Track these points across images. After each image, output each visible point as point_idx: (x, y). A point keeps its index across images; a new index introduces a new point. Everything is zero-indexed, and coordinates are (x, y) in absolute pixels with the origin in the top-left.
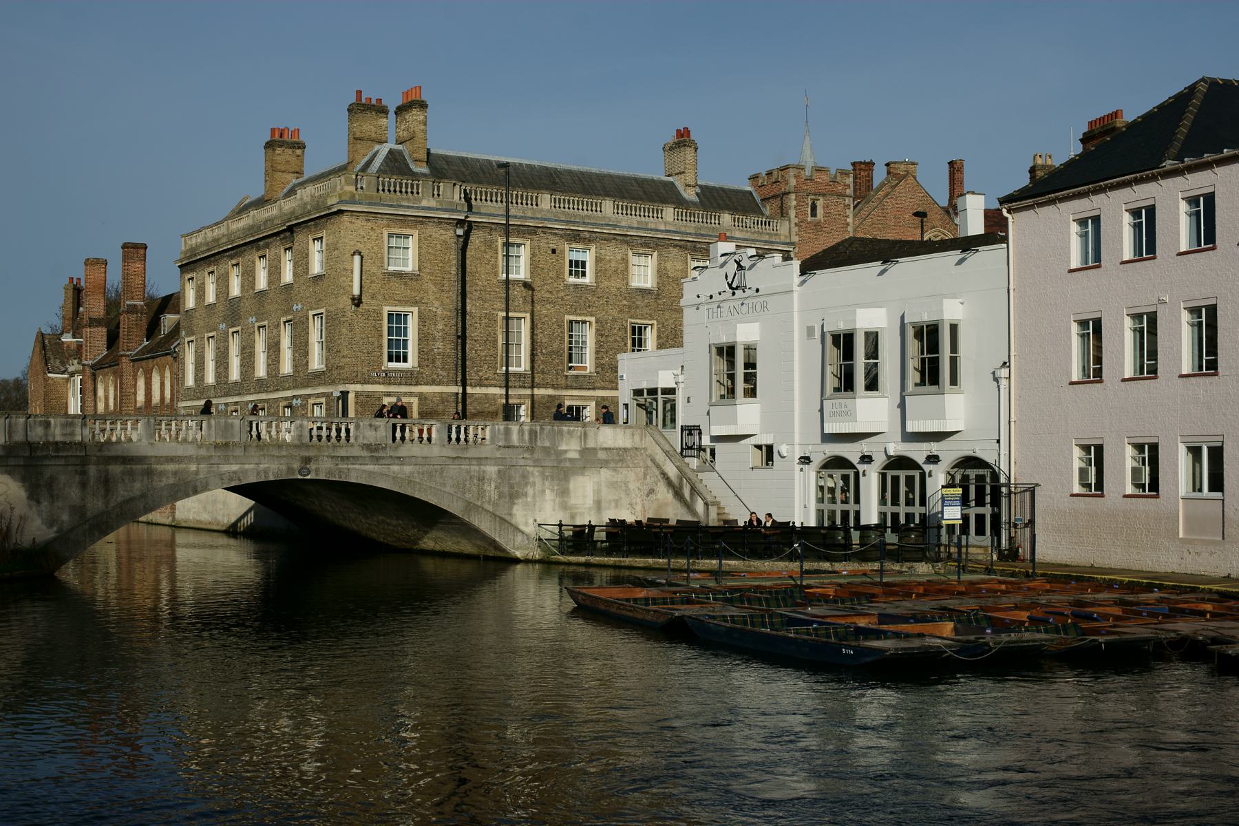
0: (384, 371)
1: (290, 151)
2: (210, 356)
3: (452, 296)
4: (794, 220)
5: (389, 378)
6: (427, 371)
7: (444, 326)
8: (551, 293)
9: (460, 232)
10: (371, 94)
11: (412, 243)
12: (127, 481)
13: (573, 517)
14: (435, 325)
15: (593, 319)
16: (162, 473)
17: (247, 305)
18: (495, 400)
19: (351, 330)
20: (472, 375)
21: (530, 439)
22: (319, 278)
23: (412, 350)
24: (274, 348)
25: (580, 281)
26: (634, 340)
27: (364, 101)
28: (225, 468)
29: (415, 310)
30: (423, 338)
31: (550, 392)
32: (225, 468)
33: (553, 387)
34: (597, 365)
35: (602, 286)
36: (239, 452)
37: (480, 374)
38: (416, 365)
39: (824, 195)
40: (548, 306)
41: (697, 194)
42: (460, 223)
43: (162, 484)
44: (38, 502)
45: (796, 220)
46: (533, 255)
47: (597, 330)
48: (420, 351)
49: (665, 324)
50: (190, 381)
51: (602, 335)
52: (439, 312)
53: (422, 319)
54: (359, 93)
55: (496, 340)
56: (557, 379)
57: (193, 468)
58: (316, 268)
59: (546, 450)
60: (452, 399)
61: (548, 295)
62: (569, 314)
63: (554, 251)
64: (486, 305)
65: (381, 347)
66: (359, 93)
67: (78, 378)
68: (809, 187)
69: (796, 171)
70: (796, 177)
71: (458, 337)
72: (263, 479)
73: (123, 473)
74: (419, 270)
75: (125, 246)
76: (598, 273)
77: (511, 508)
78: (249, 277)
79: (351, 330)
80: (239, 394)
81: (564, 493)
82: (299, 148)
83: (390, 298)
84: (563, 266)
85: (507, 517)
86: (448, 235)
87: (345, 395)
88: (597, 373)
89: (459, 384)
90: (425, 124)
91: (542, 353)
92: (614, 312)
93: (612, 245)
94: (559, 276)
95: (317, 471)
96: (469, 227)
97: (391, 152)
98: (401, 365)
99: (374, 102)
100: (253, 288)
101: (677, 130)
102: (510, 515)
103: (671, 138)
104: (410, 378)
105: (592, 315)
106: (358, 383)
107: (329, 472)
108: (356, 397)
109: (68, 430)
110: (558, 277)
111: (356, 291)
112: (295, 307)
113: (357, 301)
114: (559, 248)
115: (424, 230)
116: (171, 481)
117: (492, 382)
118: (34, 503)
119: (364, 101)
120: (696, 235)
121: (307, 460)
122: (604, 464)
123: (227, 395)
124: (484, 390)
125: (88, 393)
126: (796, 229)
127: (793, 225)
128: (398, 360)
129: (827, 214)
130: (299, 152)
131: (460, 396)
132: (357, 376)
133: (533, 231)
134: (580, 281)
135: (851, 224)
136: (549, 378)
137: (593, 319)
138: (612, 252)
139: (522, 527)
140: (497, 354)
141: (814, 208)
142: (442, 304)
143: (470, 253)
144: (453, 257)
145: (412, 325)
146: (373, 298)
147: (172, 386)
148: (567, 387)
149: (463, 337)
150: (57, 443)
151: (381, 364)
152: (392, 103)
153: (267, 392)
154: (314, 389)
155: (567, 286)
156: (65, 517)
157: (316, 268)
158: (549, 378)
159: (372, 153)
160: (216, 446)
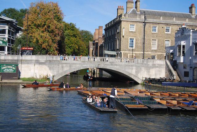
2: (110, 45)
5: (129, 50)
6: (137, 49)
9: (144, 24)
13: (150, 76)
15: (170, 40)
16: (73, 66)
22: (119, 32)
25: (168, 33)
28: (84, 65)
30: (136, 43)
31: (161, 53)
32: (84, 65)
36: (86, 63)
42: (144, 22)
44: (51, 70)
57: (78, 65)
59: (145, 64)
63: (163, 27)
65: (128, 45)
73: (66, 66)
75: (99, 27)
81: (149, 72)
86: (142, 24)
94: (163, 32)
96: (145, 23)
97: (133, 10)
107: (103, 67)
109: (56, 58)
118: (50, 70)
120: (192, 24)
121: (99, 65)
122: (157, 67)
124: (148, 53)
130: (123, 10)
134: (168, 33)
137: (170, 40)
139: (140, 78)
142: (140, 37)
143: (145, 28)
145: (134, 41)
149: (144, 43)
156: (55, 73)
160: (82, 62)
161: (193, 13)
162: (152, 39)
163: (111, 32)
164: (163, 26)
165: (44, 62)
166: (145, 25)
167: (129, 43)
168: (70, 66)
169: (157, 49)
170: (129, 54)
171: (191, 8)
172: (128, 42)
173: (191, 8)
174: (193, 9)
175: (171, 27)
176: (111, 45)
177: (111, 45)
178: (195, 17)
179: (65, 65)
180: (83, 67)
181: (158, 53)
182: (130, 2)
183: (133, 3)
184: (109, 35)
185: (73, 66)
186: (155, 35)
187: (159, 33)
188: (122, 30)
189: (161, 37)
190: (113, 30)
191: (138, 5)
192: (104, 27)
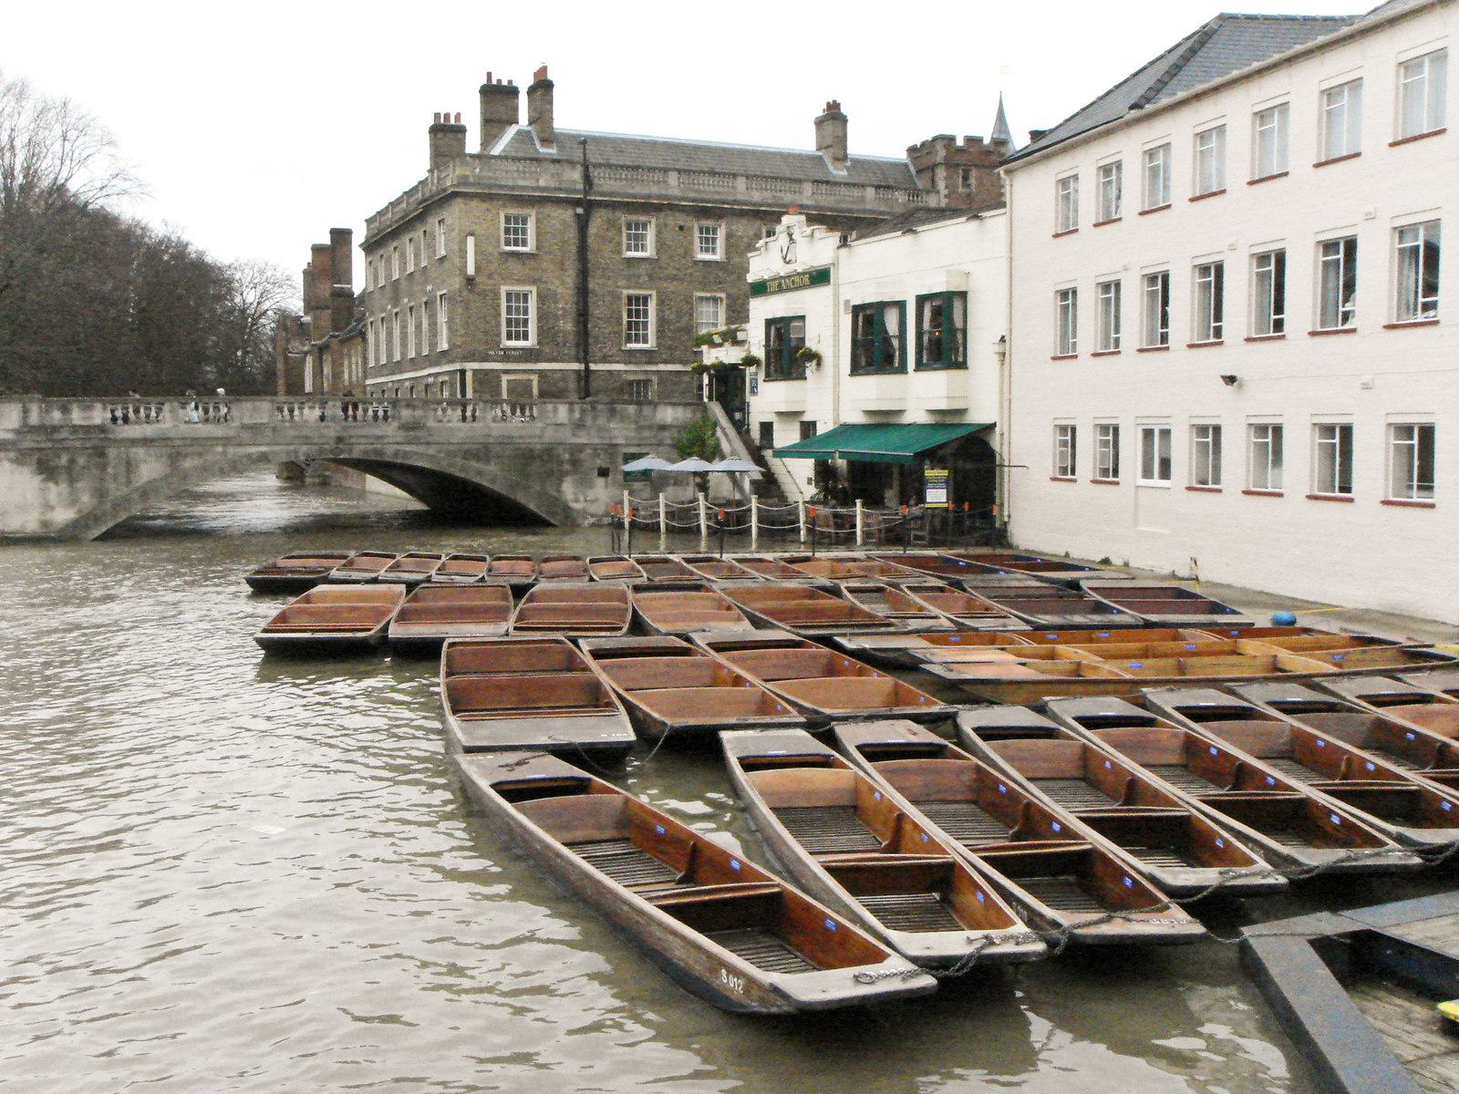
0: (502, 349)
2: (397, 333)
3: (571, 277)
4: (944, 191)
5: (507, 356)
10: (502, 76)
11: (531, 226)
15: (723, 295)
17: (404, 285)
18: (619, 376)
20: (593, 349)
24: (419, 326)
27: (494, 82)
29: (534, 289)
37: (604, 350)
39: (976, 166)
41: (848, 169)
42: (577, 203)
45: (946, 192)
50: (371, 363)
51: (734, 311)
53: (542, 298)
54: (489, 75)
55: (620, 318)
57: (220, 449)
60: (573, 376)
63: (681, 228)
64: (610, 283)
65: (498, 325)
66: (489, 75)
67: (309, 359)
69: (946, 142)
74: (538, 248)
83: (508, 278)
86: (567, 215)
87: (463, 372)
93: (744, 221)
94: (688, 252)
95: (351, 451)
96: (590, 206)
97: (519, 133)
98: (521, 344)
99: (505, 83)
102: (558, 491)
103: (819, 111)
104: (529, 355)
105: (722, 290)
106: (475, 361)
108: (474, 375)
111: (471, 270)
113: (470, 281)
114: (689, 224)
119: (494, 82)
123: (393, 373)
125: (318, 372)
128: (517, 338)
129: (980, 185)
130: (460, 136)
133: (658, 208)
137: (723, 295)
138: (743, 228)
140: (621, 331)
141: (966, 178)
142: (563, 283)
144: (572, 234)
150: (74, 426)
152: (524, 82)
155: (696, 263)
156: (86, 499)
162: (626, 292)
163: (403, 256)
164: (681, 219)
165: (10, 436)
167: (504, 316)
168: (175, 458)
170: (505, 378)
172: (497, 307)
175: (723, 226)
176: (404, 328)
177: (404, 328)
179: (139, 452)
181: (662, 367)
184: (388, 276)
186: (643, 270)
187: (664, 257)
189: (675, 278)
190: (410, 250)
192: (359, 237)
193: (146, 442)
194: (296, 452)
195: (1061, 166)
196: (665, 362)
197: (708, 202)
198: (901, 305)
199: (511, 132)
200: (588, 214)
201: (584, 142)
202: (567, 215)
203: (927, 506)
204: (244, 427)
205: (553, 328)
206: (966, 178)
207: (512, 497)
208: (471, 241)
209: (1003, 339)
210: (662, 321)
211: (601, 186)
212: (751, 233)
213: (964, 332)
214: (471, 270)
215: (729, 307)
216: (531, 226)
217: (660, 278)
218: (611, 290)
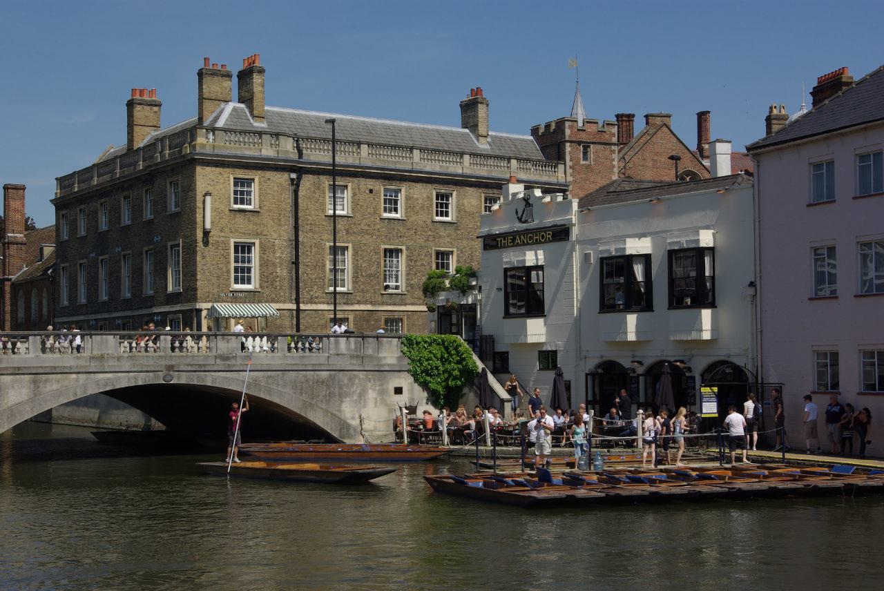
1: (148, 108)
2: (81, 280)
3: (287, 231)
5: (236, 297)
6: (267, 291)
7: (283, 253)
8: (369, 226)
10: (217, 61)
12: (16, 387)
14: (274, 252)
19: (204, 258)
20: (304, 294)
21: (356, 348)
22: (175, 216)
23: (255, 274)
24: (137, 274)
25: (393, 215)
26: (437, 264)
27: (211, 67)
29: (257, 242)
30: (264, 264)
31: (369, 307)
33: (371, 303)
34: (408, 285)
35: (411, 220)
37: (311, 293)
38: (258, 286)
39: (593, 143)
40: (367, 237)
41: (489, 143)
43: (47, 390)
45: (571, 164)
46: (354, 195)
47: (407, 256)
48: (262, 275)
49: (464, 250)
51: (411, 260)
52: (277, 242)
53: (263, 249)
55: (324, 266)
56: (375, 297)
57: (74, 376)
58: (173, 208)
61: (367, 228)
62: (384, 243)
63: (371, 191)
65: (228, 272)
68: (583, 137)
69: (570, 123)
70: (571, 127)
71: (293, 263)
72: (133, 384)
74: (260, 207)
75: (6, 188)
76: (408, 208)
77: (340, 406)
78: (115, 214)
79: (204, 258)
80: (108, 312)
82: (156, 105)
84: (379, 203)
85: (336, 413)
88: (408, 291)
89: (294, 301)
90: (263, 86)
91: (362, 275)
92: (421, 241)
93: (419, 185)
95: (179, 378)
100: (120, 224)
101: (472, 90)
102: (340, 411)
104: (252, 297)
110: (375, 213)
112: (156, 239)
115: (263, 175)
116: (55, 387)
117: (322, 300)
123: (97, 312)
124: (314, 307)
126: (569, 171)
127: (568, 168)
130: (156, 109)
131: (295, 312)
132: (208, 297)
134: (393, 215)
135: (616, 166)
136: (368, 296)
141: (585, 154)
143: (301, 193)
144: (288, 197)
145: (255, 254)
146: (221, 231)
147: (49, 305)
148: (383, 304)
149: (296, 263)
151: (229, 285)
152: (236, 67)
153: (131, 309)
154: (173, 307)
157: (173, 208)
158: (368, 296)
159: (218, 110)
161: (482, 129)
164: (371, 183)
166: (296, 184)
167: (233, 265)
169: (354, 288)
171: (469, 109)
172: (227, 257)
173: (469, 109)
174: (482, 110)
178: (488, 147)
180: (97, 382)
181: (356, 307)
182: (214, 73)
183: (229, 76)
185: (46, 381)
187: (358, 216)
188: (199, 204)
189: (366, 233)
191: (257, 89)
193: (17, 371)
194: (136, 378)
195: (818, 152)
196: (359, 303)
197: (421, 172)
198: (646, 259)
199: (229, 107)
200: (299, 178)
201: (332, 121)
202: (283, 178)
203: (703, 416)
204: (92, 358)
205: (272, 273)
206: (585, 154)
207: (303, 414)
208: (208, 199)
209: (752, 284)
210: (357, 270)
211: (309, 155)
212: (425, 196)
213: (713, 278)
214: (208, 226)
215: (409, 259)
216: (255, 188)
217: (354, 233)
218: (316, 240)
